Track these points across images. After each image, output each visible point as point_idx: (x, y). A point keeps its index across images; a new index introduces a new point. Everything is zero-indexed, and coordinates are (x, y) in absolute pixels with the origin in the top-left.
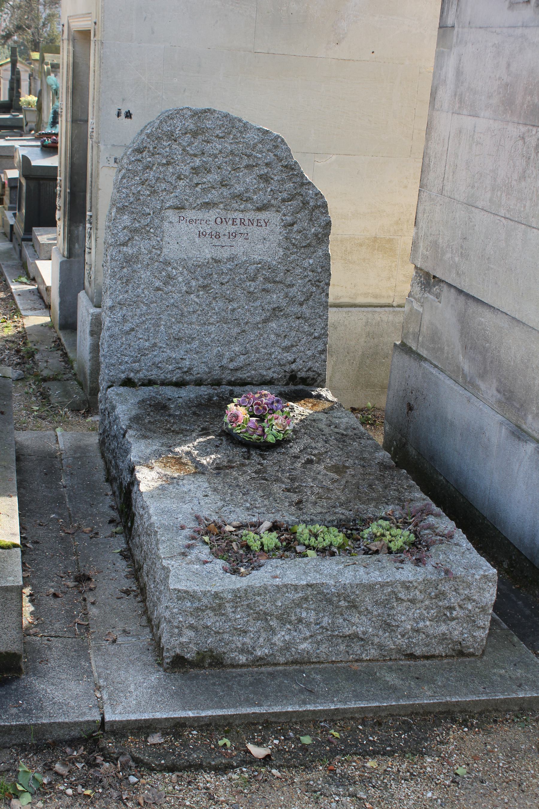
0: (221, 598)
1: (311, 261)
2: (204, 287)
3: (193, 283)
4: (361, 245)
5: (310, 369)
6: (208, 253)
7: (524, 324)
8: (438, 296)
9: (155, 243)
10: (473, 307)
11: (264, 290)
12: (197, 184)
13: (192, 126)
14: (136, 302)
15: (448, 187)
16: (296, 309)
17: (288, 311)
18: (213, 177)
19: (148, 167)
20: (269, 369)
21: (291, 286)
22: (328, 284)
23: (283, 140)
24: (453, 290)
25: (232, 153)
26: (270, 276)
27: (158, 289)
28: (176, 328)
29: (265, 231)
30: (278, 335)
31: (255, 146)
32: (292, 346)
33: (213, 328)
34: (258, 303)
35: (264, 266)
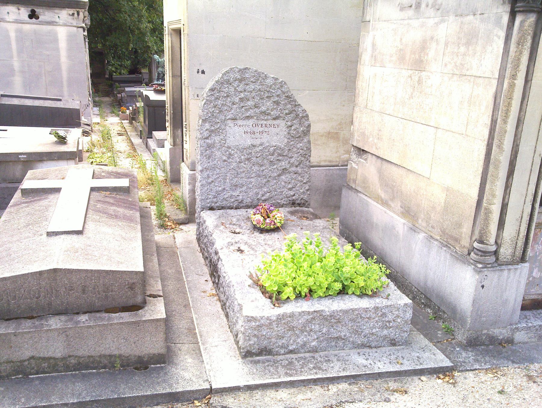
0: (270, 320)
1: (301, 145)
2: (248, 159)
3: (243, 157)
4: (322, 136)
5: (302, 199)
6: (249, 142)
7: (415, 172)
8: (366, 160)
9: (222, 137)
10: (386, 165)
11: (278, 160)
12: (243, 107)
13: (239, 77)
14: (213, 168)
15: (369, 105)
16: (294, 169)
18: (250, 103)
19: (217, 98)
20: (282, 199)
22: (310, 156)
24: (374, 157)
25: (259, 90)
26: (282, 153)
27: (225, 161)
29: (277, 130)
30: (285, 182)
32: (293, 187)
33: (253, 180)
34: (275, 167)
35: (277, 148)
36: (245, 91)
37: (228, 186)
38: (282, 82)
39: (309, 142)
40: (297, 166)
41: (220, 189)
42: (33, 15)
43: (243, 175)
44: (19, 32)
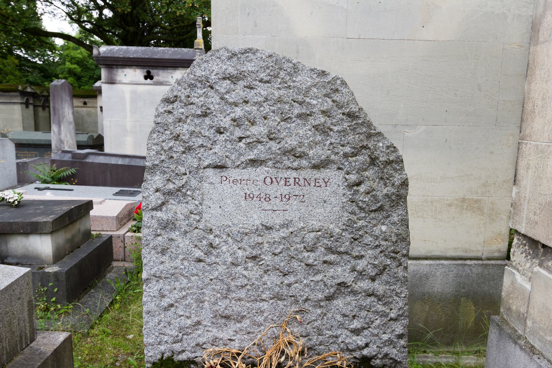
1: (384, 228)
2: (254, 258)
3: (240, 253)
4: (450, 205)
6: (256, 219)
9: (191, 207)
11: (325, 262)
12: (241, 139)
16: (365, 284)
17: (356, 287)
21: (361, 257)
23: (344, 83)
25: (279, 100)
27: (200, 261)
28: (223, 304)
29: (325, 192)
31: (308, 89)
32: (364, 328)
33: (265, 306)
34: (319, 277)
36: (246, 102)
37: (206, 316)
38: (335, 79)
39: (405, 222)
40: (373, 279)
41: (189, 322)
42: (149, 76)
43: (242, 294)
44: (133, 92)
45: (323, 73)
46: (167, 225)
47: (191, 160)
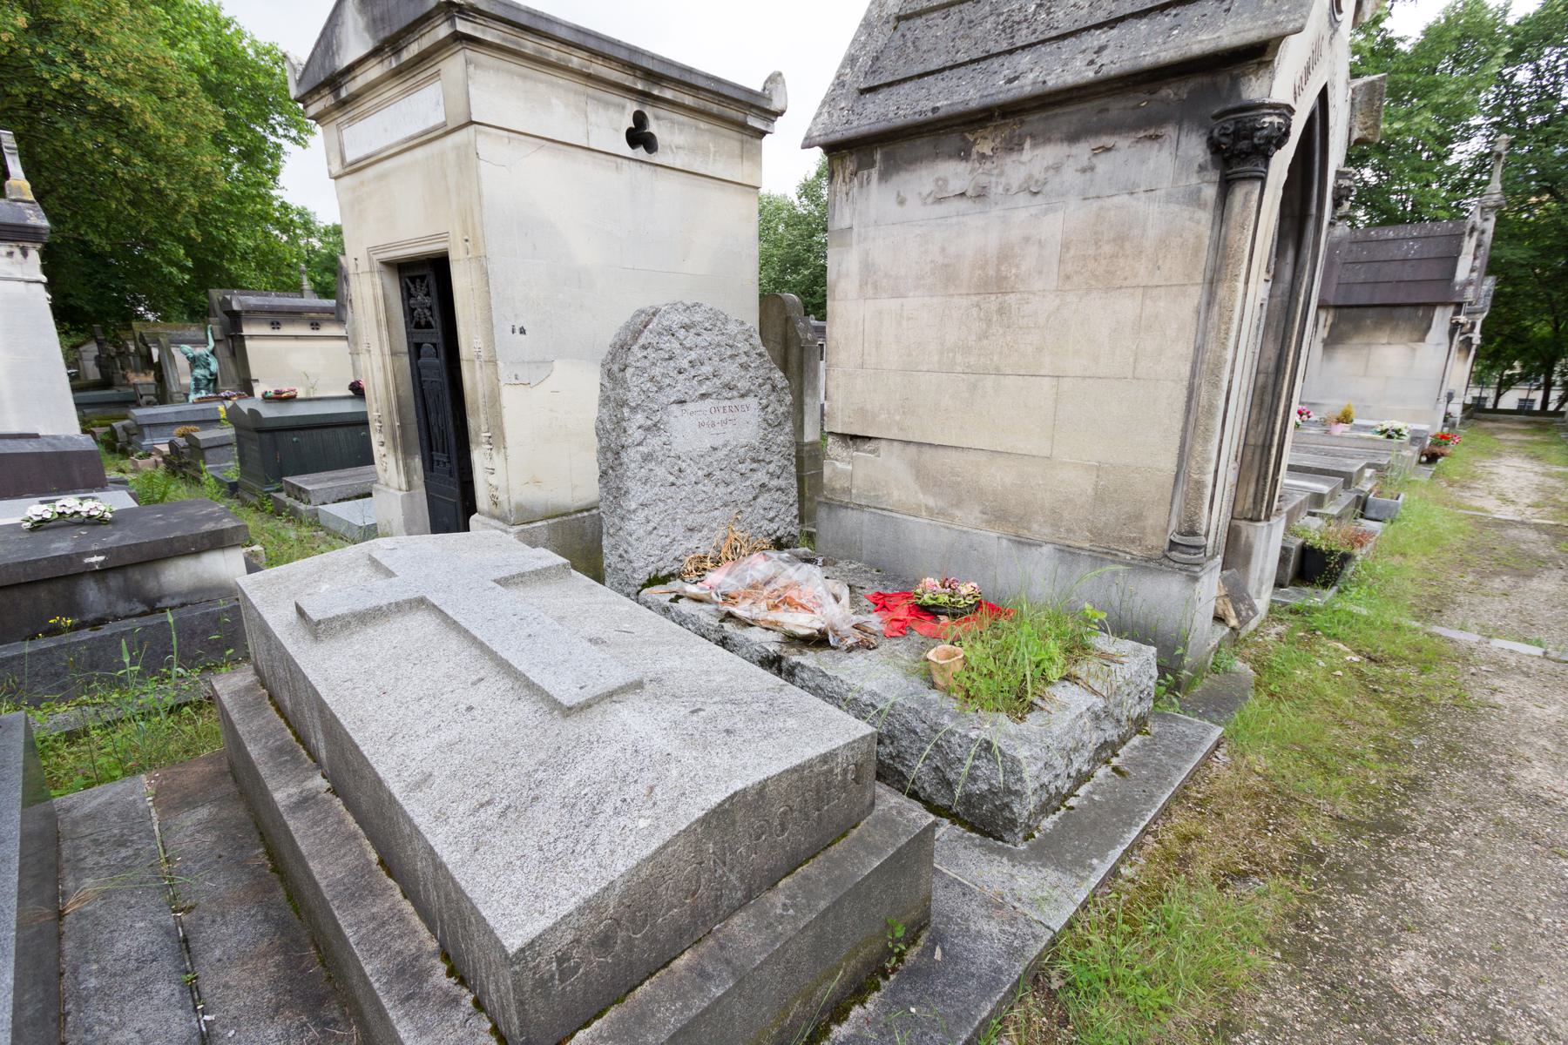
2: (709, 475)
3: (700, 473)
6: (707, 443)
9: (664, 439)
10: (928, 454)
16: (775, 483)
18: (707, 369)
25: (719, 345)
28: (690, 518)
33: (717, 513)
37: (678, 532)
43: (702, 507)
45: (742, 323)
46: (647, 458)
47: (662, 398)
